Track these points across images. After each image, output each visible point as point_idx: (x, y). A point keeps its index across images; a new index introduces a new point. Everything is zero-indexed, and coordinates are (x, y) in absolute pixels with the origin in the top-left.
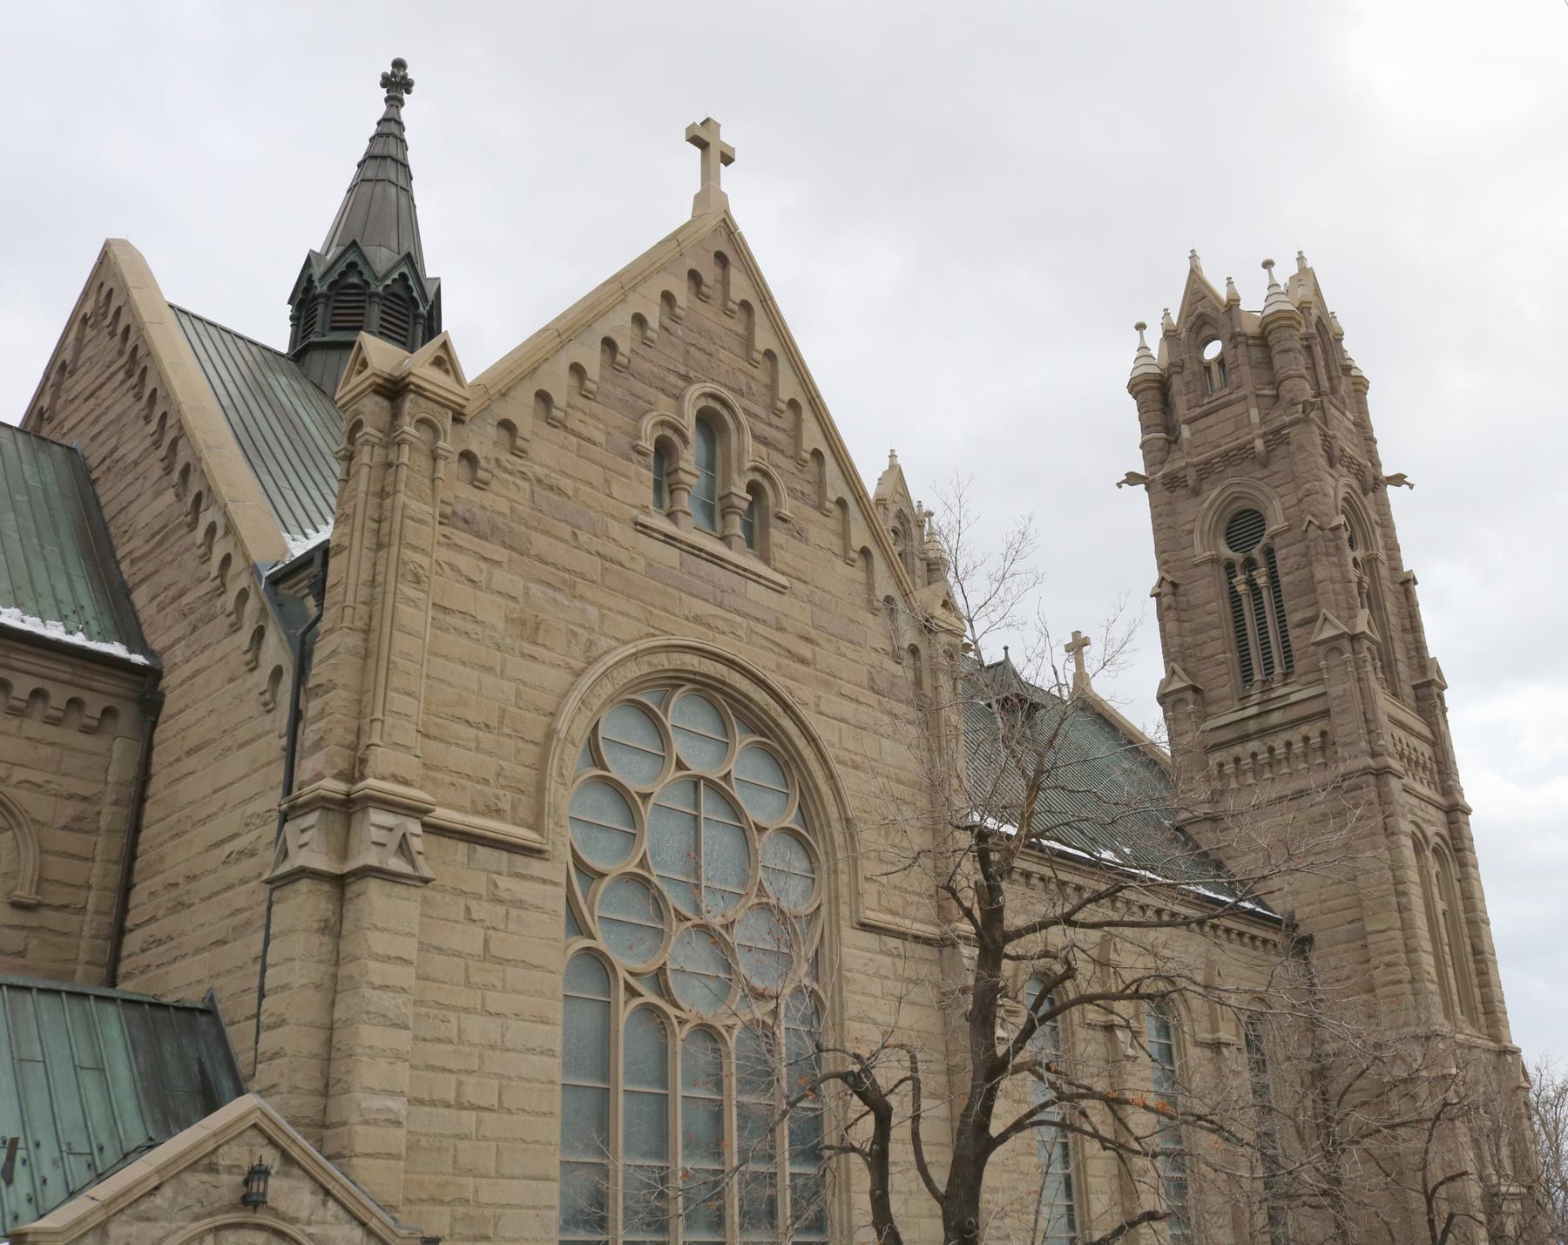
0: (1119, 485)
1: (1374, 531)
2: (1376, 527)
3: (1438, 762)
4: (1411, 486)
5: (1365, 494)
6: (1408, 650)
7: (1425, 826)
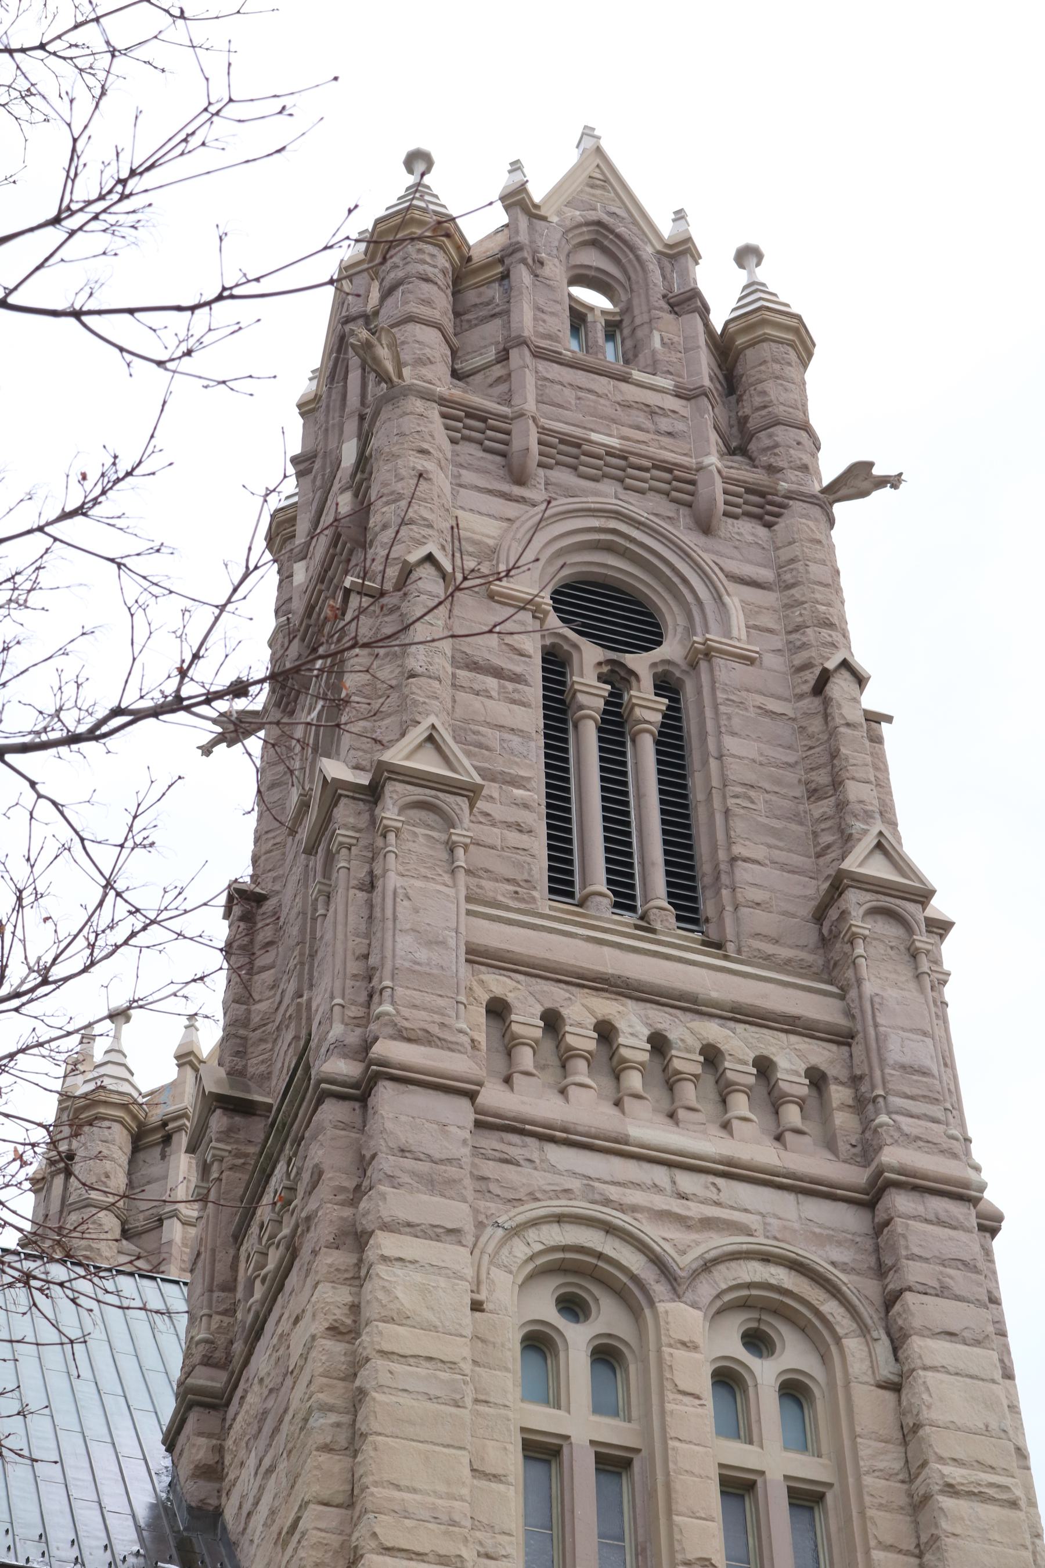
0: (207, 750)
1: (719, 599)
2: (732, 587)
3: (855, 1080)
4: (894, 482)
5: (705, 527)
6: (815, 834)
7: (654, 1233)
